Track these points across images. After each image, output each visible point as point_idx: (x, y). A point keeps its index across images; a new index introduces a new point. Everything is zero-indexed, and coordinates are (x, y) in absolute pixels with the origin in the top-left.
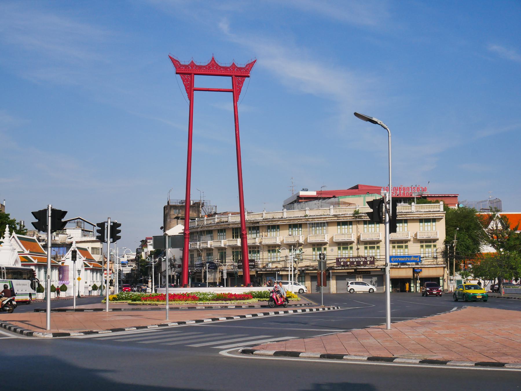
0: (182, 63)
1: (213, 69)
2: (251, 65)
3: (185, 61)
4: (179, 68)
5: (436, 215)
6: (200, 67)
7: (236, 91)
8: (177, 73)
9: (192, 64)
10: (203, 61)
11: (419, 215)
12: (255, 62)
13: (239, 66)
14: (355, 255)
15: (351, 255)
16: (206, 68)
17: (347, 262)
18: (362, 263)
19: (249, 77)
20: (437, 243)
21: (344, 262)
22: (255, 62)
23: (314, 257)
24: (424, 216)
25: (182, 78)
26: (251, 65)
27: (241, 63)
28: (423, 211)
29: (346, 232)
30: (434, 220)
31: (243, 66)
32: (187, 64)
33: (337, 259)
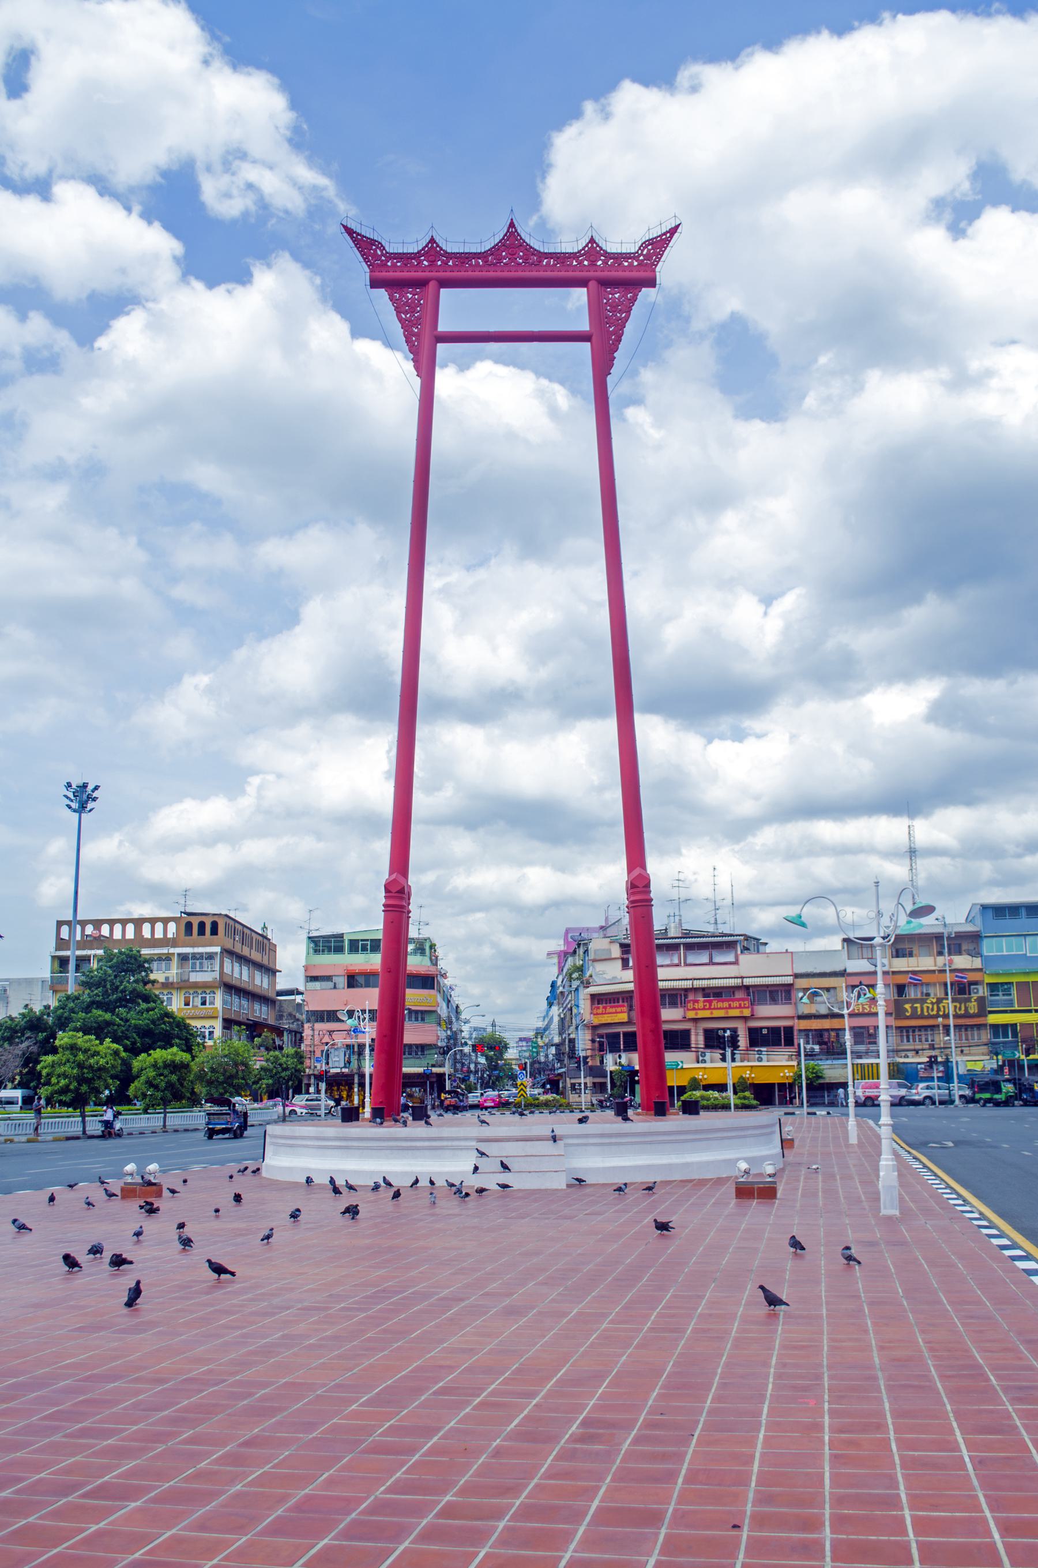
0: (391, 249)
1: (511, 262)
2: (658, 245)
3: (403, 239)
4: (384, 265)
6: (464, 258)
7: (604, 340)
8: (375, 284)
9: (432, 250)
10: (472, 235)
12: (673, 231)
13: (612, 248)
16: (486, 262)
19: (651, 283)
22: (673, 231)
25: (391, 299)
26: (658, 245)
27: (623, 239)
31: (632, 249)
32: (413, 249)
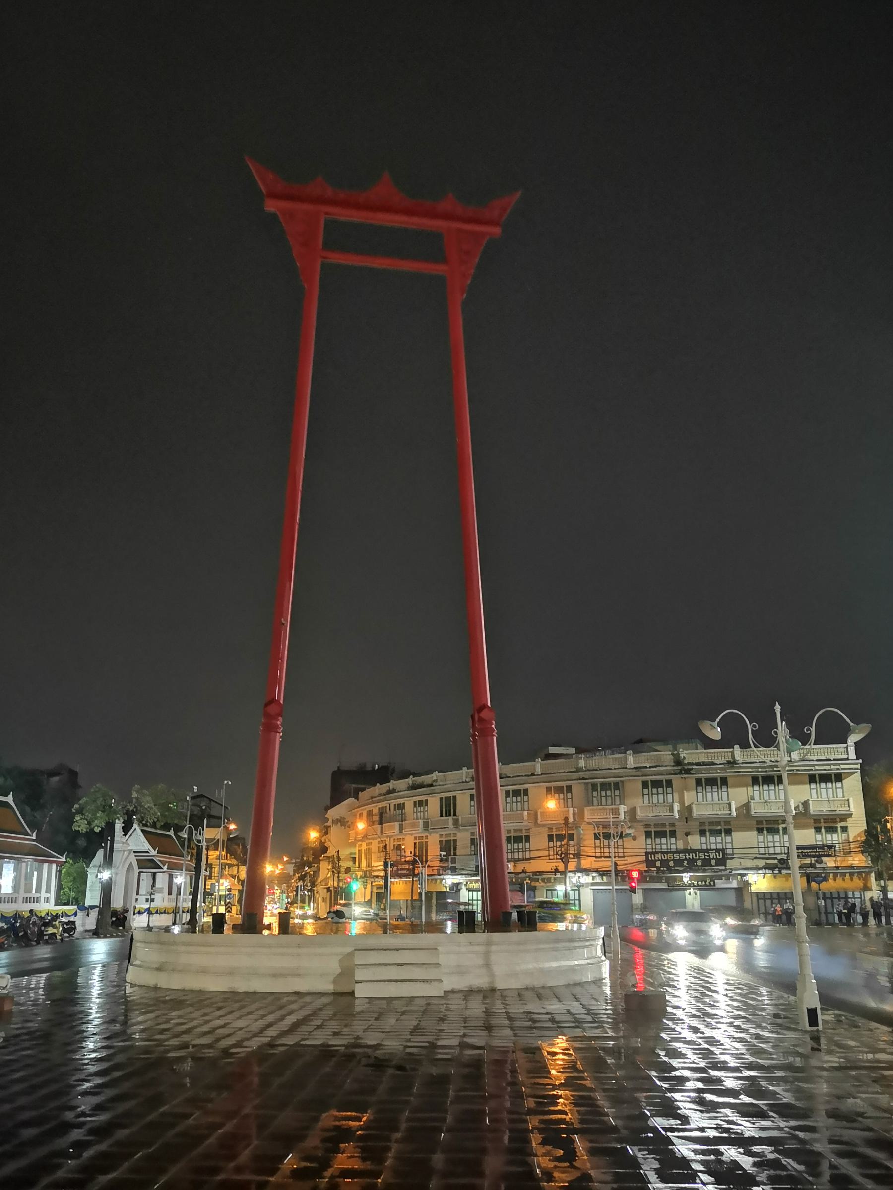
5: (842, 766)
11: (829, 767)
14: (680, 846)
15: (673, 847)
17: (668, 861)
18: (699, 863)
20: (849, 822)
21: (662, 861)
23: (598, 850)
24: (820, 769)
28: (815, 758)
29: (661, 801)
30: (839, 778)
33: (647, 854)
